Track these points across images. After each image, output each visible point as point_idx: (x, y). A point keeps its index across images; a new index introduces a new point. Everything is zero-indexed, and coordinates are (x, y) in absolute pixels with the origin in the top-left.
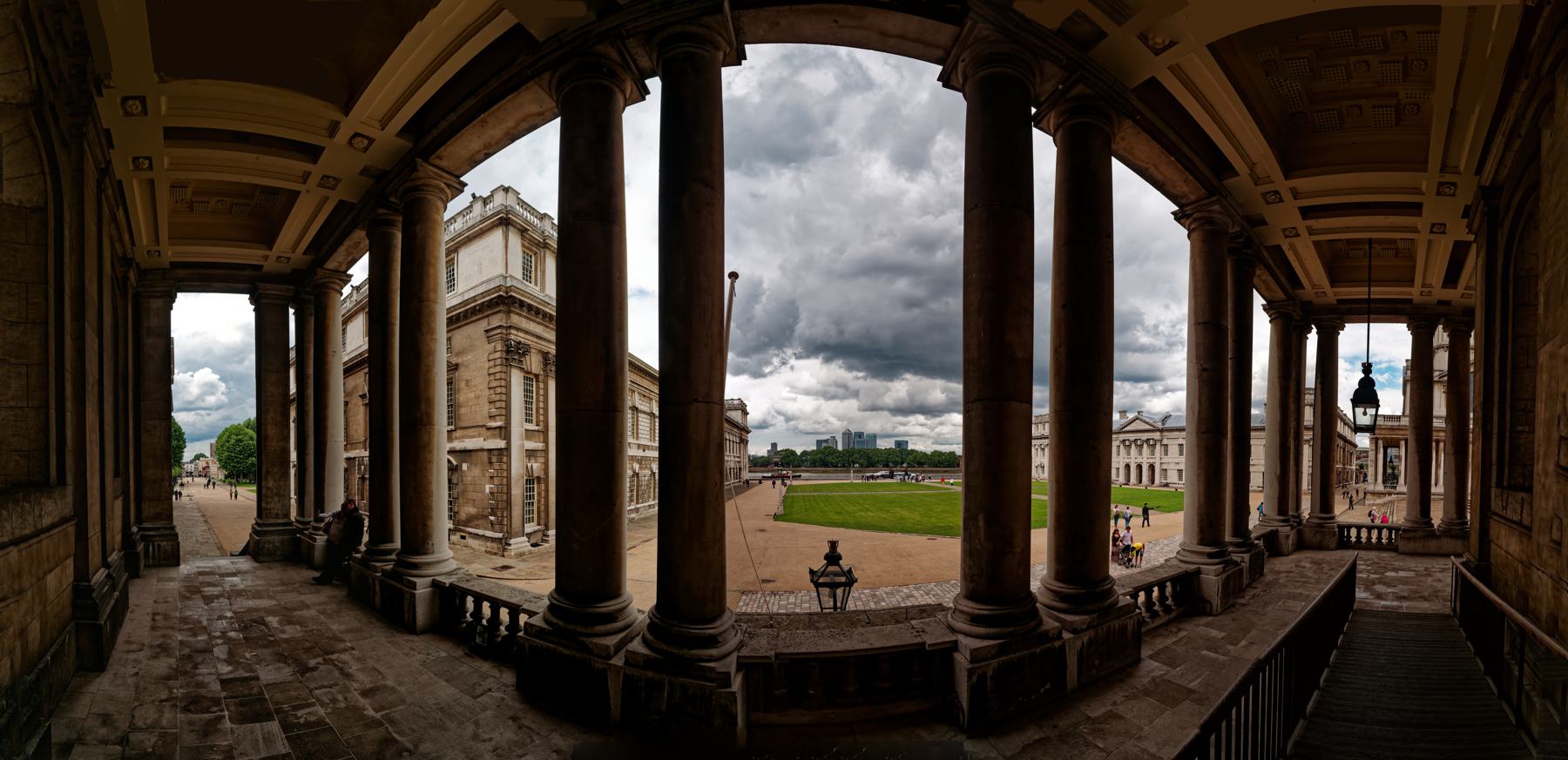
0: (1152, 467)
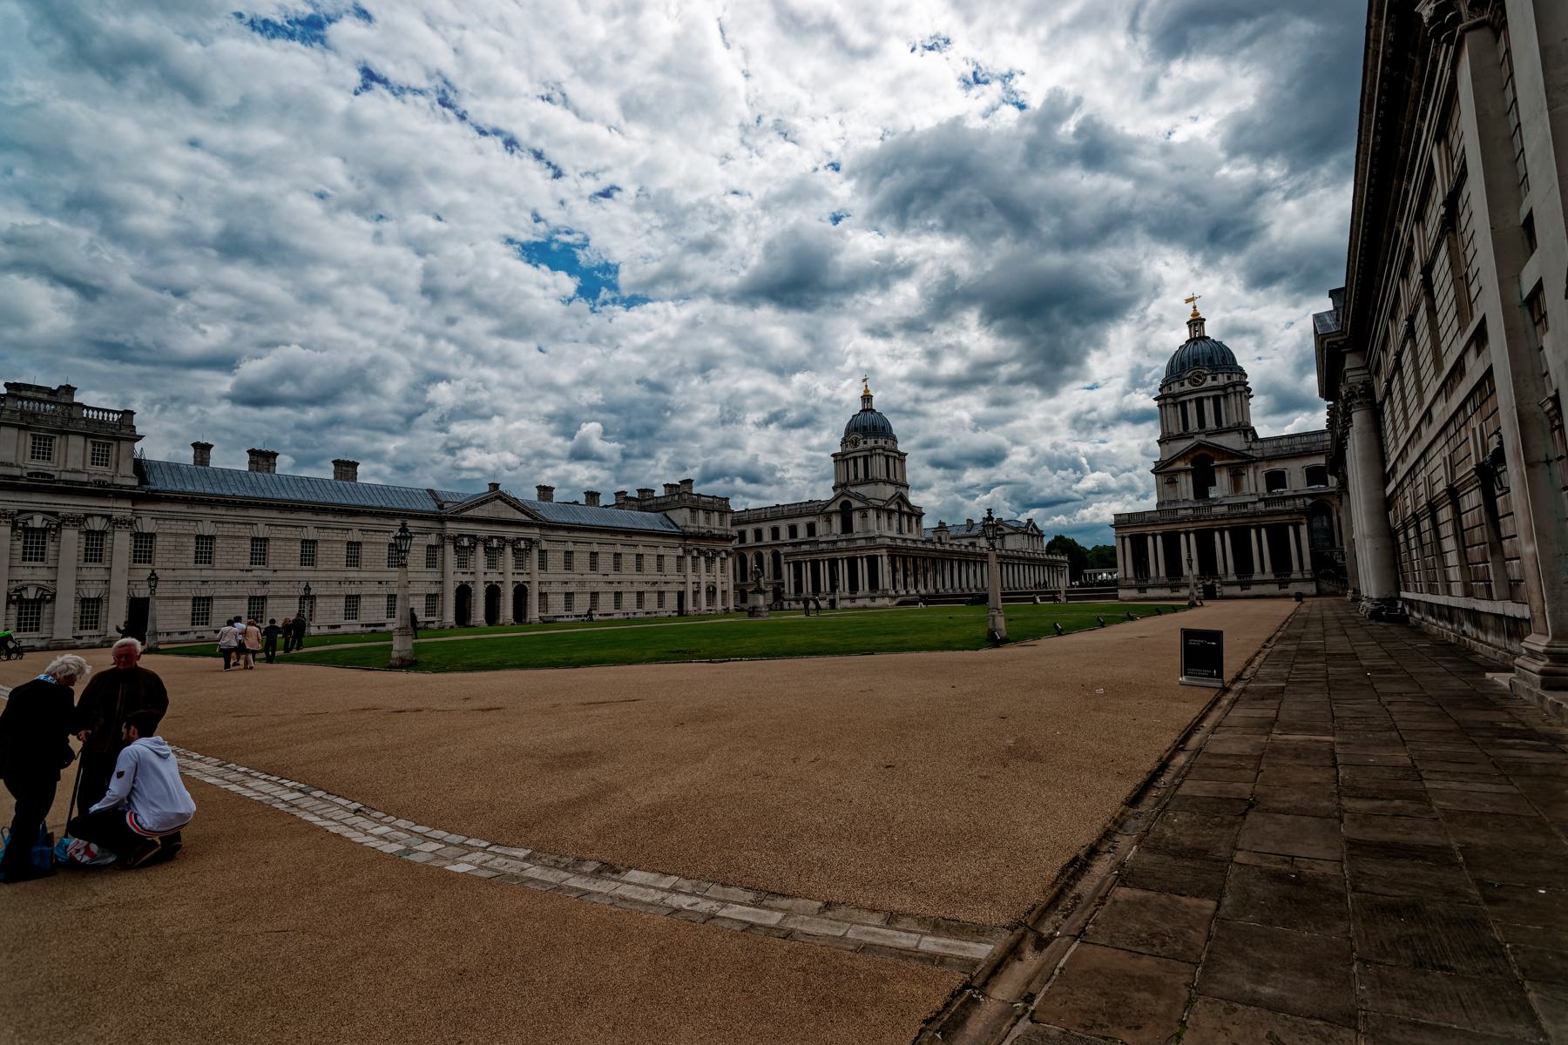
0: (521, 592)
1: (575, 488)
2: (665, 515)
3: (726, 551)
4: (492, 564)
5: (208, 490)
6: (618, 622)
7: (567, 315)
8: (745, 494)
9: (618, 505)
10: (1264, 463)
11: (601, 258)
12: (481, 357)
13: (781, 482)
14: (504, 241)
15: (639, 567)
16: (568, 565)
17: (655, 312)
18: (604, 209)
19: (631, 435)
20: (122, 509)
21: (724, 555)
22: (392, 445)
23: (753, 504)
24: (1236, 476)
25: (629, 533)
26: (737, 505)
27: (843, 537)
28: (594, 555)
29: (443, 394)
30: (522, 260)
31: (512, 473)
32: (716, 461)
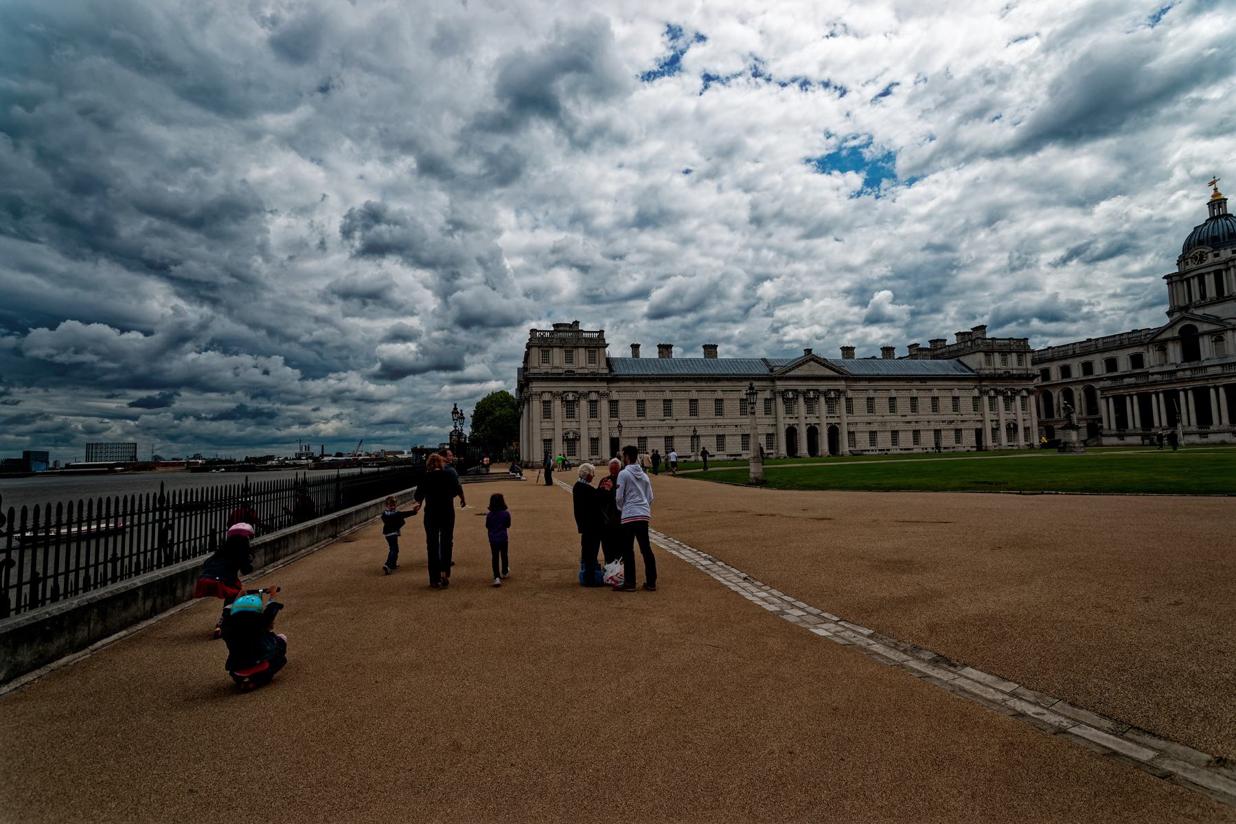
0: (833, 432)
1: (871, 346)
2: (959, 361)
3: (1027, 390)
4: (810, 410)
5: (640, 373)
6: (918, 455)
7: (857, 208)
8: (1044, 334)
9: (912, 356)
11: (884, 149)
12: (792, 256)
13: (1089, 317)
14: (804, 161)
15: (935, 408)
16: (871, 409)
17: (936, 182)
18: (884, 106)
19: (919, 295)
20: (602, 387)
21: (1025, 393)
22: (737, 330)
23: (1053, 342)
25: (923, 379)
26: (1037, 344)
27: (1186, 365)
28: (892, 400)
29: (768, 289)
30: (818, 172)
31: (821, 341)
32: (1006, 306)
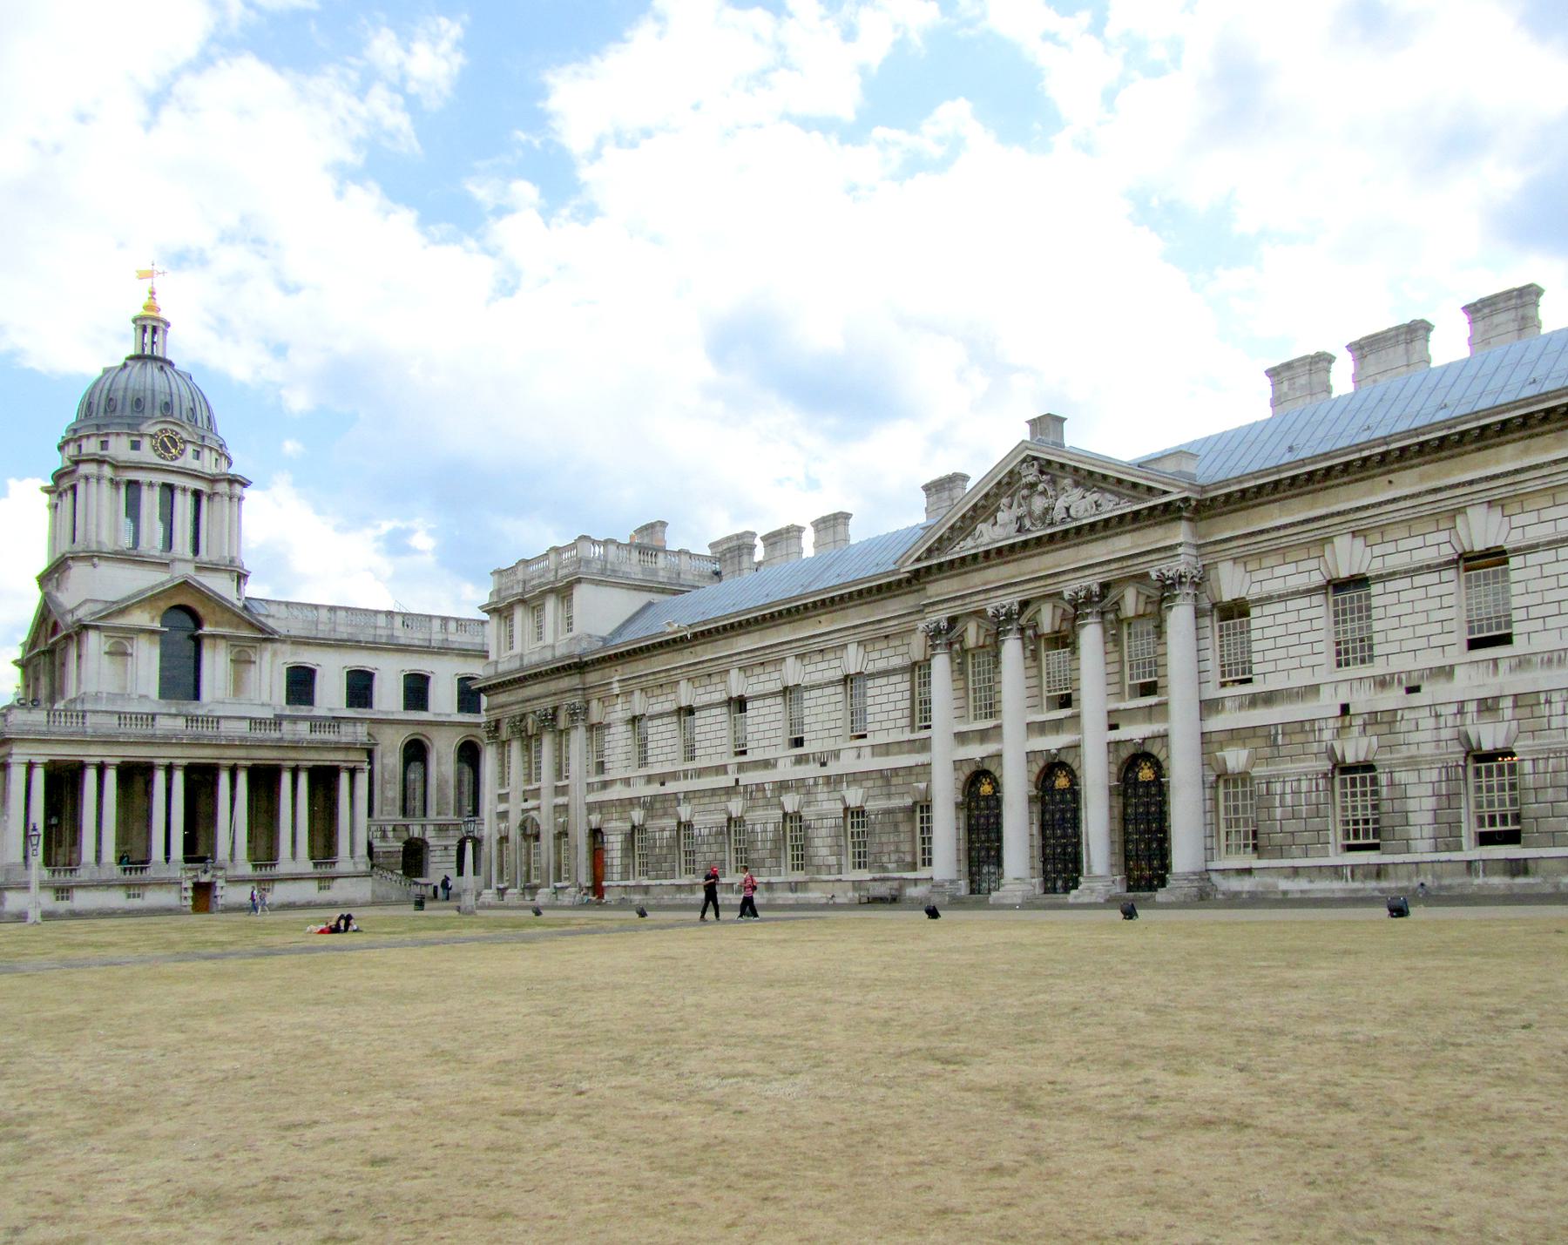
10: (287, 648)
24: (241, 662)
